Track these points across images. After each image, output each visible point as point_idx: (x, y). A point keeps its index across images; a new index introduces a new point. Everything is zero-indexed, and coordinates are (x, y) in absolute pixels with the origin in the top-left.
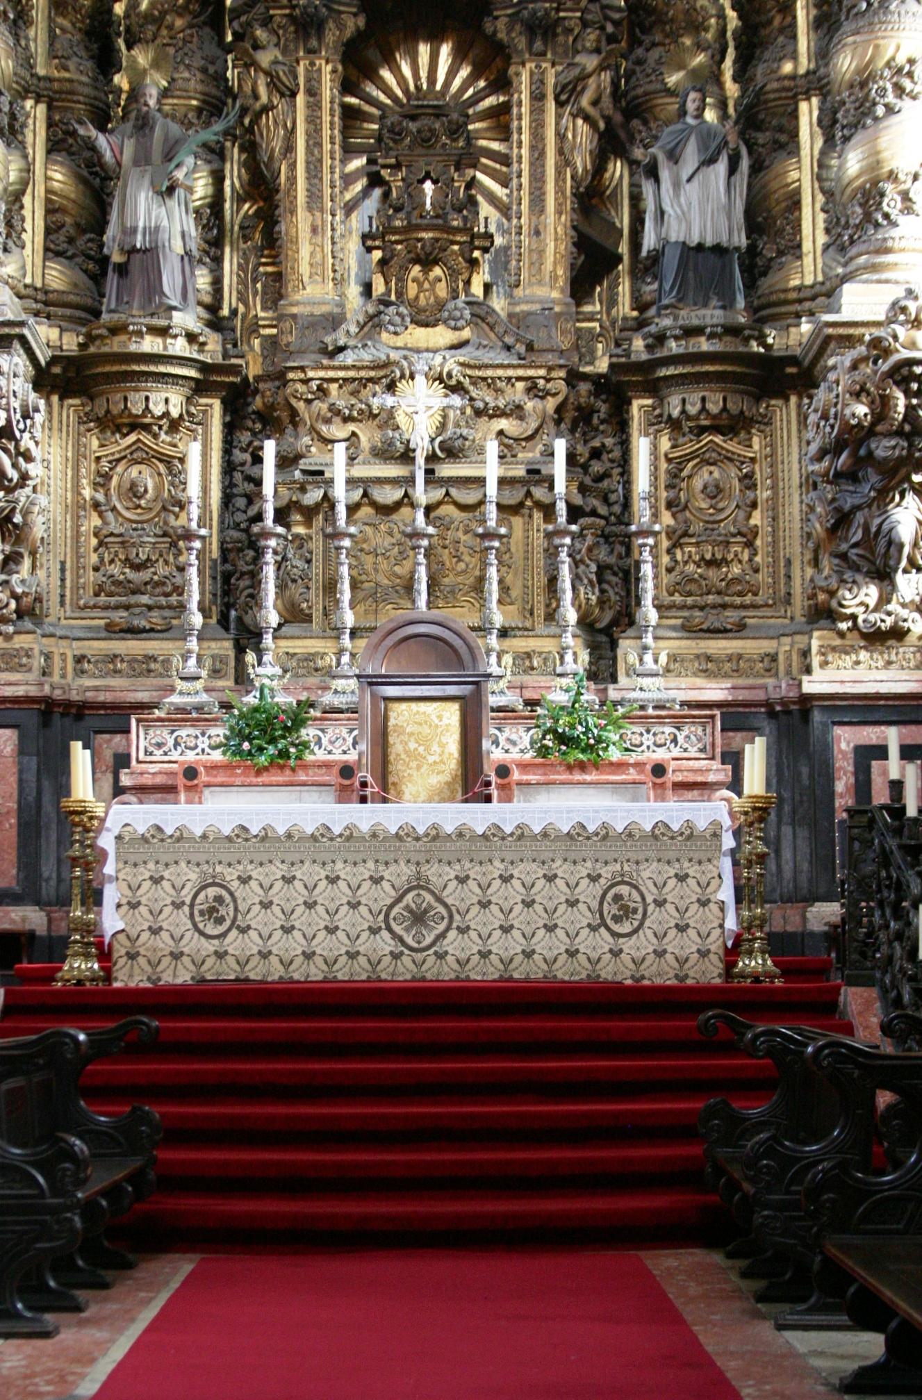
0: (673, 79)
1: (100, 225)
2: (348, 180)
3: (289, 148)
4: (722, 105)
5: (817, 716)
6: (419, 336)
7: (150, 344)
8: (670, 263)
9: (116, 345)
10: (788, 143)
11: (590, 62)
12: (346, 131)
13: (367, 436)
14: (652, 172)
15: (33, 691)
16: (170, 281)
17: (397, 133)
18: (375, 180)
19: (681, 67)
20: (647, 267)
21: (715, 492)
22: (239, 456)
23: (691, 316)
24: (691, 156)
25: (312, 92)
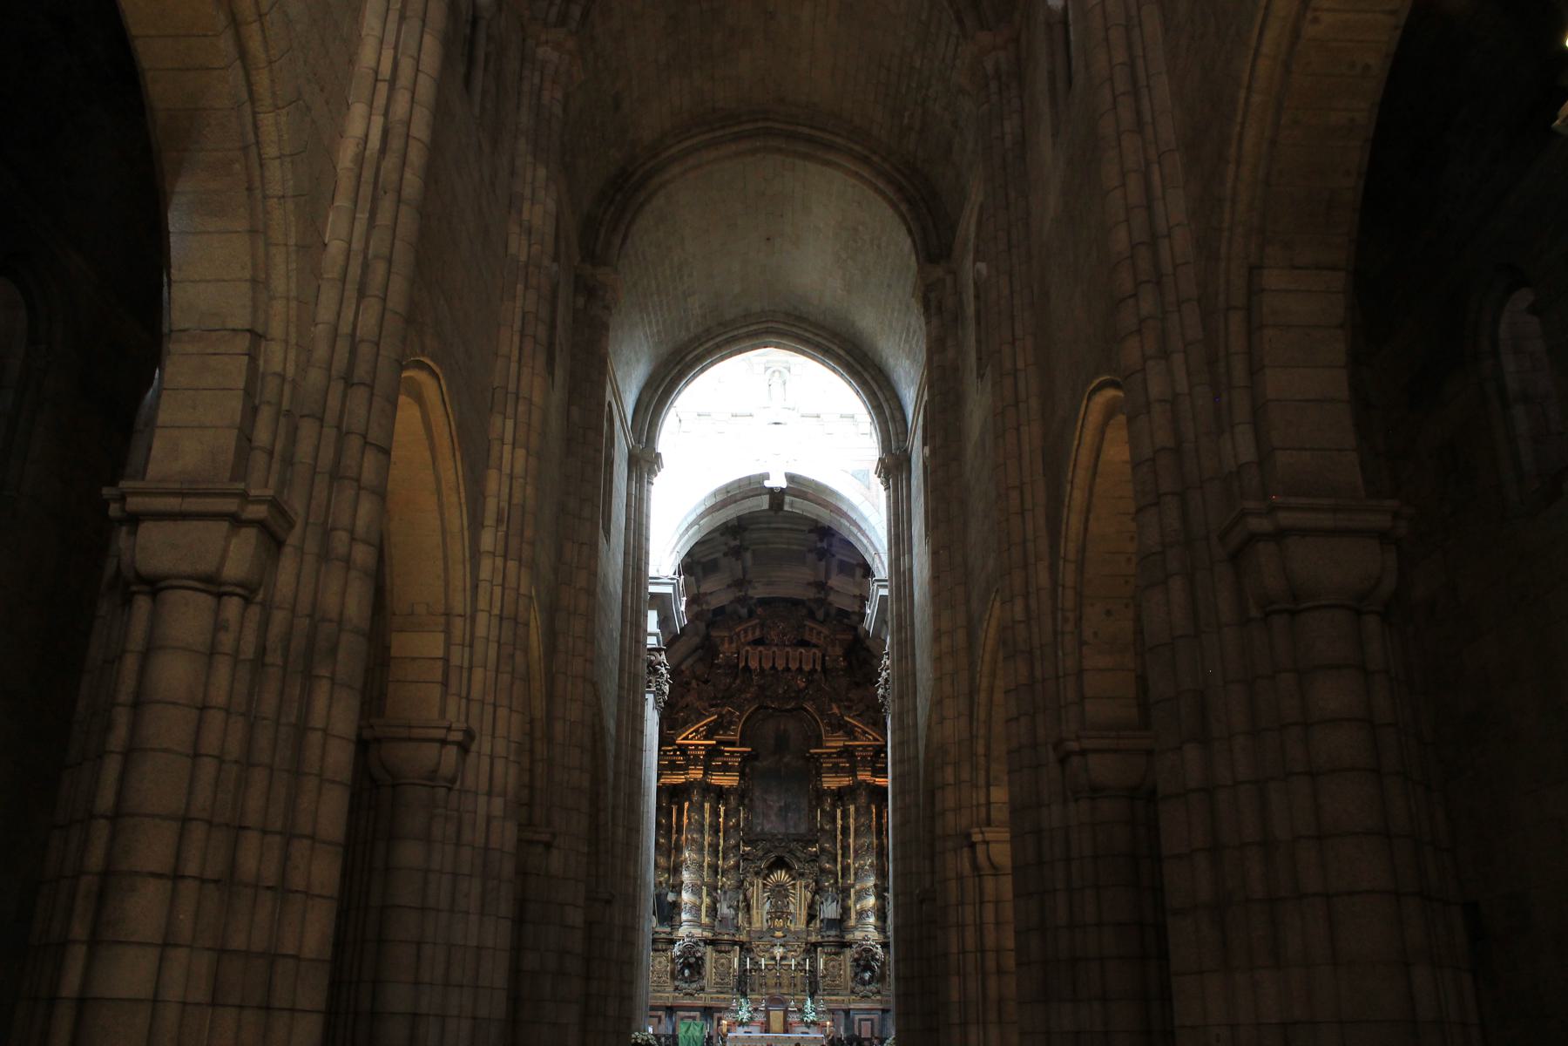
0: (826, 884)
1: (715, 910)
2: (764, 898)
3: (753, 896)
4: (837, 888)
5: (851, 1012)
6: (779, 934)
7: (726, 937)
8: (825, 922)
9: (720, 937)
10: (849, 896)
11: (811, 881)
12: (764, 888)
13: (767, 955)
14: (822, 903)
15: (702, 1005)
16: (730, 923)
17: (774, 890)
18: (769, 898)
19: (829, 881)
20: (822, 921)
21: (833, 967)
22: (742, 957)
23: (828, 933)
24: (830, 900)
25: (757, 886)
